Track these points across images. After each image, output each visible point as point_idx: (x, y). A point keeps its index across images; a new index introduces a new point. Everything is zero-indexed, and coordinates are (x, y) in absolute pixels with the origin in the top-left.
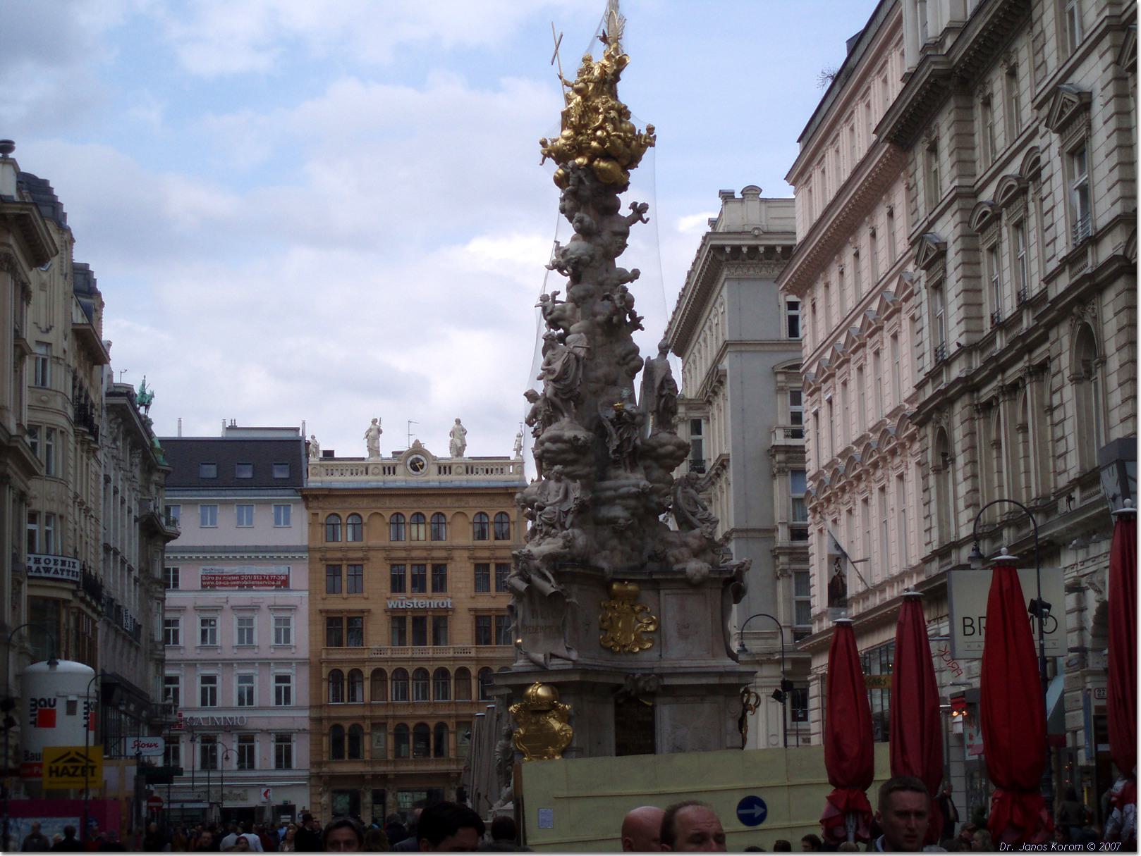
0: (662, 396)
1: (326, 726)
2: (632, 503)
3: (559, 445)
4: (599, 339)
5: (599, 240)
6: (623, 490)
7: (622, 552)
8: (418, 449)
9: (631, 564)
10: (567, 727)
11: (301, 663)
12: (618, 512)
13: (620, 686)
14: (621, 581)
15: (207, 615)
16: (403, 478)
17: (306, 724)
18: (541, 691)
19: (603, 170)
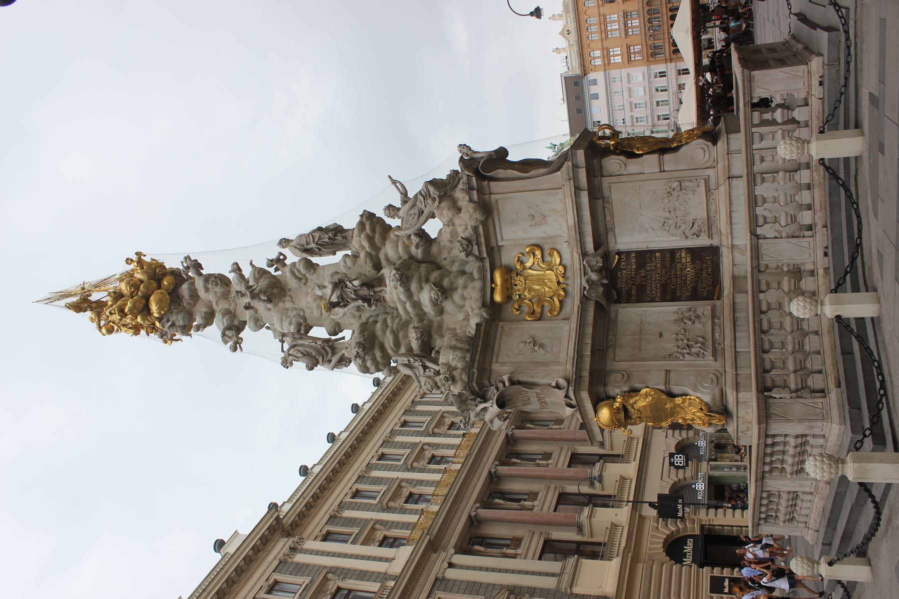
0: (320, 250)
1: (673, 56)
2: (414, 286)
3: (369, 364)
4: (288, 305)
5: (214, 306)
6: (403, 297)
7: (465, 287)
8: (562, 33)
9: (476, 276)
10: (644, 391)
11: (649, 69)
12: (426, 296)
13: (597, 304)
14: (493, 290)
15: (634, 106)
16: (573, 36)
17: (673, 64)
18: (605, 414)
19: (160, 308)
